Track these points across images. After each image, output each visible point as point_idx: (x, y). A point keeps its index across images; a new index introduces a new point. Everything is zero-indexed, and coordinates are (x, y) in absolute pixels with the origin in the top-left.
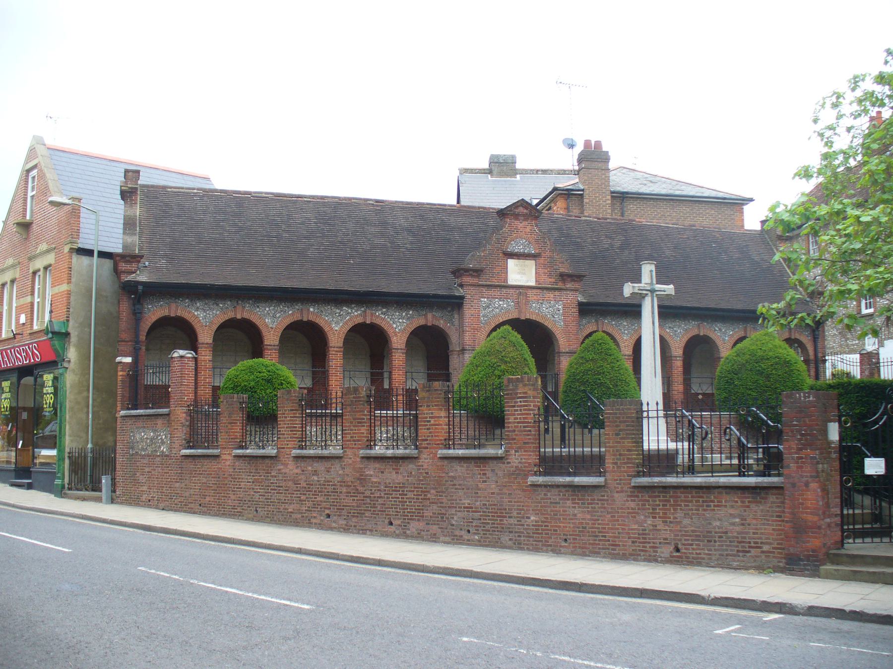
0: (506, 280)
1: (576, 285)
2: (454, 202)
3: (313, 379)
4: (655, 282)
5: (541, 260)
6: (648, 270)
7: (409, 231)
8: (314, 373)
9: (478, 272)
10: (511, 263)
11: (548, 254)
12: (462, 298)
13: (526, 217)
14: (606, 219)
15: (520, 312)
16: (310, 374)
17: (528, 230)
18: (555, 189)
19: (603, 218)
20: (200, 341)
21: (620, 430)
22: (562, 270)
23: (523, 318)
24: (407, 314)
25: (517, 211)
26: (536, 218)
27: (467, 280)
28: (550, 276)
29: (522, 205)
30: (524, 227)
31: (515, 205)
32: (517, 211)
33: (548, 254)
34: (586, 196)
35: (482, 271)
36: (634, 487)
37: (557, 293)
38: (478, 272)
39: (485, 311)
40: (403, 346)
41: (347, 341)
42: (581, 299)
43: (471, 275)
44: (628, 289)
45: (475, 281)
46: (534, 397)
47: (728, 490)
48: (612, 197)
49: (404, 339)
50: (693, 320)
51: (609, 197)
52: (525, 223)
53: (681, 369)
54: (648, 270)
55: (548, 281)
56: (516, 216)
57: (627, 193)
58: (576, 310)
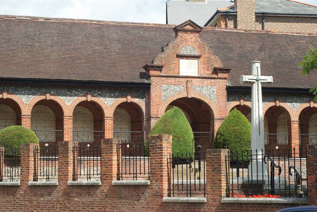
0: (179, 73)
1: (225, 75)
2: (165, 23)
3: (95, 137)
4: (259, 74)
5: (202, 59)
6: (257, 66)
7: (119, 41)
8: (95, 133)
9: (160, 68)
10: (183, 62)
11: (207, 55)
12: (149, 84)
13: (192, 32)
14: (251, 31)
15: (188, 93)
16: (93, 135)
17: (193, 40)
18: (218, 12)
19: (249, 30)
20: (65, 115)
21: (215, 168)
22: (216, 66)
23: (190, 97)
24: (114, 95)
25: (186, 28)
26: (199, 32)
27: (152, 73)
28: (208, 70)
29: (189, 24)
30: (191, 38)
31: (185, 24)
32: (186, 28)
33: (207, 55)
34: (239, 16)
35: (162, 67)
36: (223, 204)
37: (212, 80)
38: (160, 68)
39: (164, 93)
40: (112, 116)
41: (115, 113)
42: (229, 84)
43: (155, 70)
44: (246, 78)
45: (158, 73)
46: (167, 148)
47: (277, 206)
48: (256, 16)
49: (113, 111)
50: (306, 97)
51: (254, 16)
52: (191, 35)
53: (297, 130)
54: (257, 66)
55: (209, 73)
56: (186, 31)
57: (266, 13)
58: (225, 92)
